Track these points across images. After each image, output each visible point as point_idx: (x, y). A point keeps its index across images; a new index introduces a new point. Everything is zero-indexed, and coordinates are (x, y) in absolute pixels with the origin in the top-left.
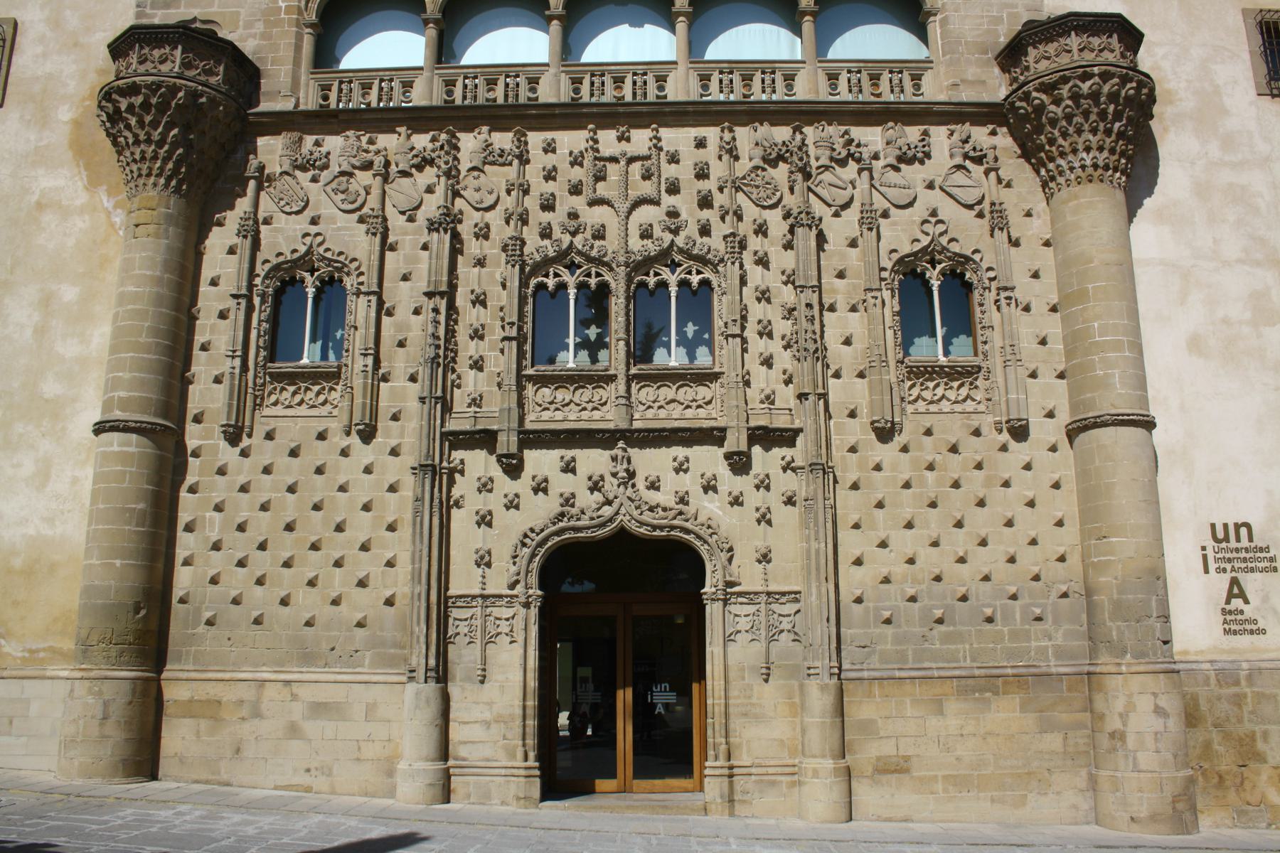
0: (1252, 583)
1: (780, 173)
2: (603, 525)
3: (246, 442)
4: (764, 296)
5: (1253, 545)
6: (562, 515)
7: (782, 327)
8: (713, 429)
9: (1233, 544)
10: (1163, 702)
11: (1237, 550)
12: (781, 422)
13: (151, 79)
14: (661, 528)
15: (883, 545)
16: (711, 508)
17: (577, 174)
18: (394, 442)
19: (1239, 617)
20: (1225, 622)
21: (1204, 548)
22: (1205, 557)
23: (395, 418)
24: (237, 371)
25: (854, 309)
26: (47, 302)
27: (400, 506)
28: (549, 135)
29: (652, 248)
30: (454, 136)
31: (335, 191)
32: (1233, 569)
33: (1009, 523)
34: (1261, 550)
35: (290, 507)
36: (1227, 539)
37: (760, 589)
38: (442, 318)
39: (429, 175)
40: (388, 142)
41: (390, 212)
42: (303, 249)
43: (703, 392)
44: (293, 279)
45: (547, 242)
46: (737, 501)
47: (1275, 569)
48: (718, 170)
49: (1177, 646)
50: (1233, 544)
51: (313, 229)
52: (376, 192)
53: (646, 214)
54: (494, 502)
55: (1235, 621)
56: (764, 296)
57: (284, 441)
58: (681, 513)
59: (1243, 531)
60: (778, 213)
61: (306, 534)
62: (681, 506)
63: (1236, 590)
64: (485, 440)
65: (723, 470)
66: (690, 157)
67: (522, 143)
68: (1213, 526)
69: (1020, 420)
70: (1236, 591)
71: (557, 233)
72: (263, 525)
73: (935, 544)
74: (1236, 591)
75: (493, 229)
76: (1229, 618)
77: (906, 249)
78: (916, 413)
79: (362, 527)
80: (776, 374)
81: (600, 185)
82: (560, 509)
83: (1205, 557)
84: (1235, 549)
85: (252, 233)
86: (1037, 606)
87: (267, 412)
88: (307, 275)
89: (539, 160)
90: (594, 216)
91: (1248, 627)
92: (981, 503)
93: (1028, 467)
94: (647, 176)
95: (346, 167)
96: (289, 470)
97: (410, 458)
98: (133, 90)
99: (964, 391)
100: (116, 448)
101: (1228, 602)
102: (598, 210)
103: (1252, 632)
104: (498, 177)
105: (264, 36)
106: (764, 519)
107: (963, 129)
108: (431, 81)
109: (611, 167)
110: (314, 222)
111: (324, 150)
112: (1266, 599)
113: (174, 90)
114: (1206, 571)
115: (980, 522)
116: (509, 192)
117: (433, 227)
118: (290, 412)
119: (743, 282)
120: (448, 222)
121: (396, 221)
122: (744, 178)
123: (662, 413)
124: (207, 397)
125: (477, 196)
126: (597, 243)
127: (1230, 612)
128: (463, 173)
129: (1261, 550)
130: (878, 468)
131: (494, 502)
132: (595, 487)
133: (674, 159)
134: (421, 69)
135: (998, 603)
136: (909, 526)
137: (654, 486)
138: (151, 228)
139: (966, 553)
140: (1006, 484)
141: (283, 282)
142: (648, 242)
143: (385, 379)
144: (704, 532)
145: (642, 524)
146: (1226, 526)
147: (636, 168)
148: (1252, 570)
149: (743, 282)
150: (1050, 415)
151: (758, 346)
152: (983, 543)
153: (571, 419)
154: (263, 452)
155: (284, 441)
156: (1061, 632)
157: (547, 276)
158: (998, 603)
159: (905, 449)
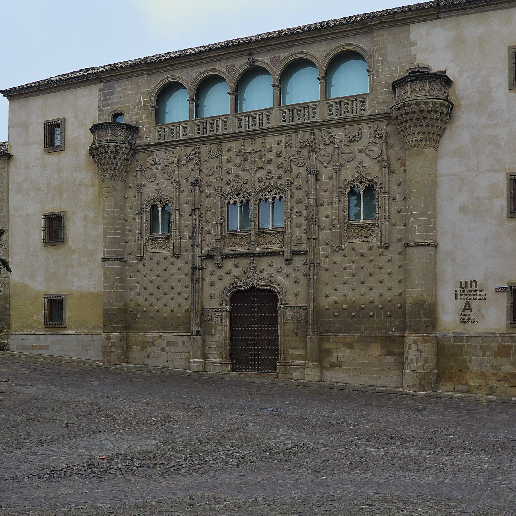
0: (474, 304)
1: (305, 152)
2: (246, 285)
3: (144, 262)
4: (299, 202)
5: (477, 289)
6: (235, 282)
7: (304, 213)
8: (280, 252)
9: (469, 289)
10: (421, 347)
11: (470, 291)
12: (303, 248)
13: (101, 144)
14: (264, 285)
15: (335, 290)
16: (281, 278)
17: (238, 159)
18: (186, 259)
19: (468, 317)
20: (461, 318)
21: (456, 291)
22: (456, 294)
23: (186, 251)
24: (140, 239)
25: (329, 204)
26: (85, 218)
27: (187, 281)
28: (228, 145)
29: (262, 186)
30: (199, 148)
31: (164, 173)
32: (467, 299)
33: (381, 282)
34: (480, 291)
35: (159, 282)
36: (466, 287)
37: (294, 305)
38: (197, 217)
39: (190, 166)
40: (180, 152)
41: (181, 178)
42: (155, 195)
43: (280, 238)
44: (155, 204)
45: (228, 187)
46: (287, 276)
47: (485, 299)
48: (284, 155)
49: (441, 327)
50: (469, 289)
51: (159, 187)
52: (176, 172)
53: (261, 174)
54: (214, 278)
55: (466, 318)
56: (299, 202)
57: (155, 260)
58: (270, 281)
59: (473, 284)
60: (305, 168)
61: (162, 290)
62: (271, 278)
63: (468, 307)
64: (211, 257)
65: (283, 265)
66: (276, 149)
67: (220, 149)
68: (461, 282)
69: (385, 244)
70: (467, 307)
71: (232, 184)
72: (151, 288)
73: (353, 290)
74: (467, 307)
75: (213, 183)
76: (463, 317)
77: (350, 179)
78: (350, 242)
79: (179, 287)
80: (302, 230)
81: (246, 162)
82: (234, 280)
83: (456, 294)
84: (469, 291)
85: (140, 189)
86: (389, 312)
87: (150, 251)
88: (158, 203)
89: (227, 155)
90: (244, 176)
91: (470, 320)
92: (371, 275)
93: (389, 261)
94: (261, 158)
95: (166, 164)
96: (158, 270)
97: (190, 265)
98: (97, 148)
99: (369, 233)
100: (107, 267)
101: (463, 311)
102: (246, 173)
103: (472, 322)
104: (213, 163)
105: (138, 114)
106: (296, 282)
107: (374, 125)
108: (191, 126)
109: (249, 156)
110: (158, 185)
111: (159, 158)
112: (479, 310)
113: (109, 147)
114: (456, 299)
115: (371, 282)
116: (217, 168)
117: (193, 185)
118: (156, 251)
119: (291, 197)
120: (197, 183)
121: (184, 182)
122: (293, 156)
123: (266, 246)
124: (131, 246)
125: (207, 171)
126: (245, 186)
127: (464, 315)
128: (202, 163)
129: (480, 291)
130: (335, 263)
131: (214, 278)
132: (244, 273)
133: (270, 150)
134: (188, 121)
135: (375, 310)
136: (345, 283)
137: (262, 272)
138: (109, 194)
139: (365, 293)
140: (380, 268)
141: (152, 206)
142: (261, 184)
143: (182, 238)
144: (277, 287)
145: (258, 284)
146: (466, 282)
147: (257, 155)
148: (475, 299)
149: (291, 197)
150: (399, 241)
151: (297, 220)
152: (371, 289)
153: (238, 249)
154: (151, 265)
155: (155, 260)
156: (398, 321)
157: (230, 199)
158: (375, 310)
159: (344, 256)
